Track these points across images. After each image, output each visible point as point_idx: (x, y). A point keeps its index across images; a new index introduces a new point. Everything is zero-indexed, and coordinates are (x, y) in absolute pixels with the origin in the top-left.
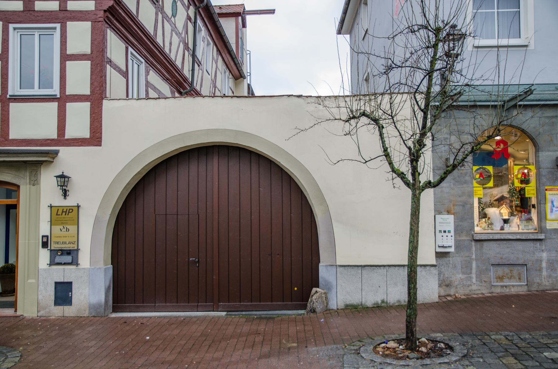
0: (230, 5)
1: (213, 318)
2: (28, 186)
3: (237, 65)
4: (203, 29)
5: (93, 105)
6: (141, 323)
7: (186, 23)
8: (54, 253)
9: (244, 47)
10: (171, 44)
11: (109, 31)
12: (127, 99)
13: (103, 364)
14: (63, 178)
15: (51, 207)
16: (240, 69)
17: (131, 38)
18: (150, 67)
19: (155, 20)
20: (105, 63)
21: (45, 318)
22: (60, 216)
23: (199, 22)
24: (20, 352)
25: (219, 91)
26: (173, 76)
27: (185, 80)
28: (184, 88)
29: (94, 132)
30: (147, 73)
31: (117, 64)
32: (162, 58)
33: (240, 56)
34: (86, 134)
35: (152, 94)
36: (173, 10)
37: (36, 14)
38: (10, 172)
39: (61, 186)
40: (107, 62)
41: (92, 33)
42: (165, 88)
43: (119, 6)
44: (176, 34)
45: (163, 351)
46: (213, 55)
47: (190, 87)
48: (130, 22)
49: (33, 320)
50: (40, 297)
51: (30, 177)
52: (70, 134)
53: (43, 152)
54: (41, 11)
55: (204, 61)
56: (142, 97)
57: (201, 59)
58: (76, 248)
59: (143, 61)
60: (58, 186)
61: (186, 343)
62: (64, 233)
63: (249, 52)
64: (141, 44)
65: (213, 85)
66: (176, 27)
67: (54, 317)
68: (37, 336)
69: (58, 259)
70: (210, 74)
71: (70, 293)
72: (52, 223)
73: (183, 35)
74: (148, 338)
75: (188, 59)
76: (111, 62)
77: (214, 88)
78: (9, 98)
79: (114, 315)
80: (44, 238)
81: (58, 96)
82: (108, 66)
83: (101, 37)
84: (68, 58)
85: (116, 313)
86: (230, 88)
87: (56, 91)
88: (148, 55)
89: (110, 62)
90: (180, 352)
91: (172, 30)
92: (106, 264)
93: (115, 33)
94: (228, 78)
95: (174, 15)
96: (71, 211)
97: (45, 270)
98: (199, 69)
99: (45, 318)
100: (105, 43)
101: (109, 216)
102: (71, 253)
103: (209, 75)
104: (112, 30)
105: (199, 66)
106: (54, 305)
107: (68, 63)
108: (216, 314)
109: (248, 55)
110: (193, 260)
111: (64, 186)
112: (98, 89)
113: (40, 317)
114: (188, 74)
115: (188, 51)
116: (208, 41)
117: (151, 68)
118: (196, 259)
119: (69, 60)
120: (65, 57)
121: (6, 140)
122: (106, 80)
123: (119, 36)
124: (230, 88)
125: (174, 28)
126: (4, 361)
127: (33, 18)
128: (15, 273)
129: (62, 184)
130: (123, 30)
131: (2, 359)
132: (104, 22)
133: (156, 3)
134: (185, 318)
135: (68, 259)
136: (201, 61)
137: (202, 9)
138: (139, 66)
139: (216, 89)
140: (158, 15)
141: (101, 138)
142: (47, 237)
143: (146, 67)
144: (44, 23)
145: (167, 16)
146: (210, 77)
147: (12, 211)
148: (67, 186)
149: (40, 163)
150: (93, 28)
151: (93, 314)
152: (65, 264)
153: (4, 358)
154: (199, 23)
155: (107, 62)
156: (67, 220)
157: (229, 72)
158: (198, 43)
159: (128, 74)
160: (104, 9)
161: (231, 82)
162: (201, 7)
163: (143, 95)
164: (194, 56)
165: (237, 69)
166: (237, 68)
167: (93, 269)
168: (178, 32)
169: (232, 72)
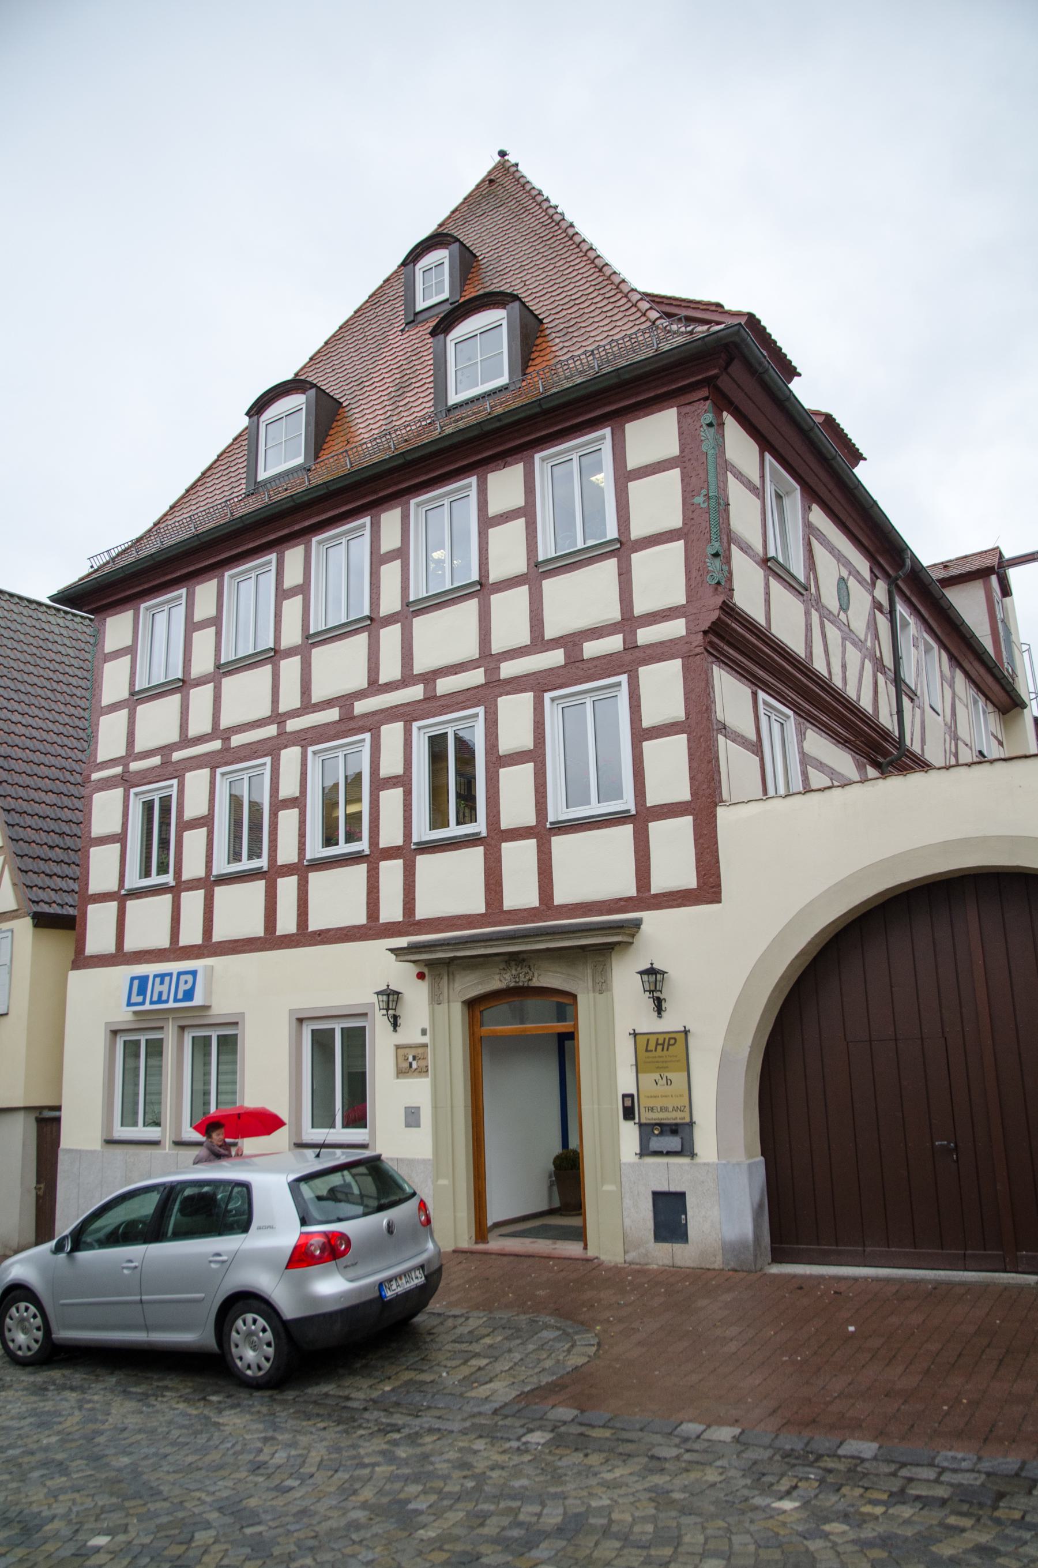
0: (966, 557)
1: (1006, 1288)
2: (591, 995)
3: (1002, 681)
4: (911, 620)
5: (699, 821)
6: (835, 1293)
7: (872, 617)
8: (646, 1130)
9: (1014, 638)
10: (844, 667)
11: (715, 669)
12: (764, 798)
13: (757, 1382)
14: (652, 974)
15: (635, 1035)
16: (1008, 689)
17: (761, 673)
18: (806, 722)
19: (806, 626)
20: (715, 733)
21: (638, 1267)
22: (654, 1054)
23: (901, 608)
24: (596, 1335)
25: (967, 745)
26: (858, 733)
27: (885, 734)
28: (886, 753)
29: (705, 875)
30: (801, 736)
31: (738, 730)
32: (828, 699)
33: (1005, 660)
34: (689, 880)
35: (817, 779)
36: (841, 596)
37: (585, 666)
38: (559, 970)
39: (650, 991)
40: (719, 731)
41: (685, 678)
42: (843, 761)
43: (731, 616)
44: (854, 644)
45: (887, 1365)
46: (941, 671)
47: (898, 749)
48: (755, 642)
49: (616, 1269)
50: (627, 1222)
51: (593, 976)
52: (659, 884)
53: (612, 925)
54: (594, 659)
55: (922, 687)
56: (795, 791)
57: (916, 685)
58: (687, 1120)
59: (790, 713)
60: (645, 991)
61: (942, 1349)
62: (662, 1088)
63: (1028, 647)
64: (781, 680)
65: (950, 736)
66: (851, 630)
67: (655, 1267)
68: (625, 1305)
69: (655, 1144)
70: (940, 711)
71: (683, 1217)
72: (639, 1068)
73: (869, 644)
74: (851, 1329)
75: (887, 690)
76: (725, 728)
77: (953, 742)
78: (550, 829)
79: (776, 1269)
80: (626, 1099)
81: (633, 812)
82: (721, 739)
83: (703, 684)
84: (646, 736)
85: (779, 1265)
86: (992, 734)
87: (627, 803)
88: (799, 700)
89: (723, 728)
90: (928, 1371)
91: (844, 639)
92: (749, 1155)
93: (729, 669)
94: (984, 712)
95: (844, 607)
96: (672, 1042)
97: (631, 1165)
98: (913, 708)
99: (638, 1267)
100: (712, 693)
101: (749, 1049)
102: (680, 1130)
103: (939, 715)
104: (722, 665)
105: (912, 700)
106: (653, 1240)
107: (646, 745)
108: (1013, 1278)
109: (1026, 655)
110: (941, 1145)
111: (655, 990)
112: (705, 787)
113: (630, 1264)
114: (890, 722)
115: (884, 673)
116: (926, 643)
117: (808, 725)
118: (949, 1143)
119: (646, 740)
120: (640, 735)
121: (549, 908)
122: (719, 766)
123: (736, 674)
124: (992, 734)
125: (848, 634)
126: (569, 1351)
127: (581, 673)
128: (579, 1168)
129: (653, 988)
130: (743, 660)
131: (567, 1346)
132: (706, 654)
133: (804, 593)
134: (938, 1284)
135: (673, 1143)
136: (916, 689)
137: (903, 580)
138: (782, 724)
139: (960, 743)
140: (811, 615)
141: (719, 885)
142: (632, 1096)
143: (798, 725)
144: (599, 679)
145: (830, 612)
146: (940, 719)
147: (567, 1043)
148: (661, 991)
149: (610, 947)
150: (686, 669)
151: (732, 1265)
152: (669, 1154)
153: (570, 1344)
154: (900, 612)
155: (717, 730)
156: (666, 1062)
157: (984, 699)
158: (903, 652)
159: (761, 746)
160: (703, 629)
161: (992, 722)
162: (900, 577)
163: (797, 785)
164: (898, 681)
165: (1002, 691)
166: (1003, 688)
167: (724, 1164)
168: (857, 640)
169: (993, 699)
